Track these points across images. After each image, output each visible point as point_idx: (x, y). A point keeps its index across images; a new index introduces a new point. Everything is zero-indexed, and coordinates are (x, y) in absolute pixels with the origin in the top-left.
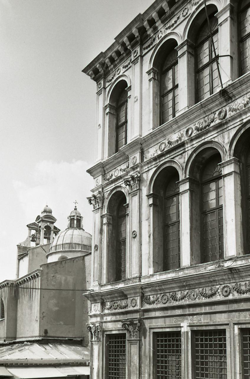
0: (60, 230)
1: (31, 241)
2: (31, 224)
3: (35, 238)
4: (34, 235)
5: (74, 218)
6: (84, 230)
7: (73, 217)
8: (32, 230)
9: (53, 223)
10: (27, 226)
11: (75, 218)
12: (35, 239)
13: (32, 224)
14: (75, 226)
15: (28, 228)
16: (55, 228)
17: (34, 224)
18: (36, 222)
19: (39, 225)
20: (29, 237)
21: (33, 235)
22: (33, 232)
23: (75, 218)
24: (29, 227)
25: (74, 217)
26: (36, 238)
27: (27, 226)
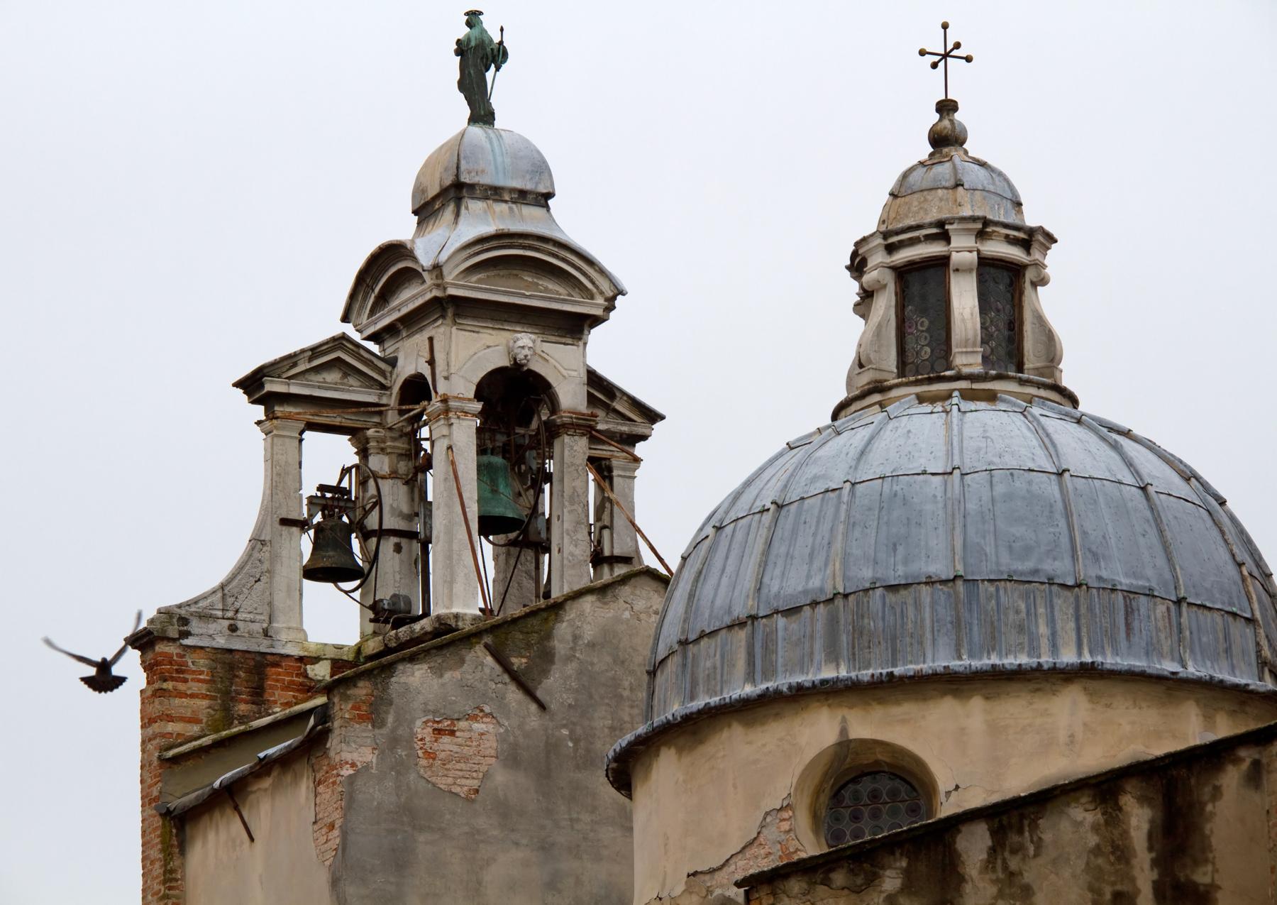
0: (653, 417)
1: (312, 573)
2: (291, 359)
3: (349, 529)
4: (336, 489)
5: (942, 262)
6: (1074, 401)
7: (935, 249)
8: (308, 435)
10: (251, 385)
11: (963, 249)
12: (356, 544)
13: (315, 351)
14: (968, 360)
15: (259, 411)
18: (349, 330)
19: (393, 362)
20: (285, 522)
24: (269, 401)
25: (945, 237)
26: (365, 535)
27: (251, 385)
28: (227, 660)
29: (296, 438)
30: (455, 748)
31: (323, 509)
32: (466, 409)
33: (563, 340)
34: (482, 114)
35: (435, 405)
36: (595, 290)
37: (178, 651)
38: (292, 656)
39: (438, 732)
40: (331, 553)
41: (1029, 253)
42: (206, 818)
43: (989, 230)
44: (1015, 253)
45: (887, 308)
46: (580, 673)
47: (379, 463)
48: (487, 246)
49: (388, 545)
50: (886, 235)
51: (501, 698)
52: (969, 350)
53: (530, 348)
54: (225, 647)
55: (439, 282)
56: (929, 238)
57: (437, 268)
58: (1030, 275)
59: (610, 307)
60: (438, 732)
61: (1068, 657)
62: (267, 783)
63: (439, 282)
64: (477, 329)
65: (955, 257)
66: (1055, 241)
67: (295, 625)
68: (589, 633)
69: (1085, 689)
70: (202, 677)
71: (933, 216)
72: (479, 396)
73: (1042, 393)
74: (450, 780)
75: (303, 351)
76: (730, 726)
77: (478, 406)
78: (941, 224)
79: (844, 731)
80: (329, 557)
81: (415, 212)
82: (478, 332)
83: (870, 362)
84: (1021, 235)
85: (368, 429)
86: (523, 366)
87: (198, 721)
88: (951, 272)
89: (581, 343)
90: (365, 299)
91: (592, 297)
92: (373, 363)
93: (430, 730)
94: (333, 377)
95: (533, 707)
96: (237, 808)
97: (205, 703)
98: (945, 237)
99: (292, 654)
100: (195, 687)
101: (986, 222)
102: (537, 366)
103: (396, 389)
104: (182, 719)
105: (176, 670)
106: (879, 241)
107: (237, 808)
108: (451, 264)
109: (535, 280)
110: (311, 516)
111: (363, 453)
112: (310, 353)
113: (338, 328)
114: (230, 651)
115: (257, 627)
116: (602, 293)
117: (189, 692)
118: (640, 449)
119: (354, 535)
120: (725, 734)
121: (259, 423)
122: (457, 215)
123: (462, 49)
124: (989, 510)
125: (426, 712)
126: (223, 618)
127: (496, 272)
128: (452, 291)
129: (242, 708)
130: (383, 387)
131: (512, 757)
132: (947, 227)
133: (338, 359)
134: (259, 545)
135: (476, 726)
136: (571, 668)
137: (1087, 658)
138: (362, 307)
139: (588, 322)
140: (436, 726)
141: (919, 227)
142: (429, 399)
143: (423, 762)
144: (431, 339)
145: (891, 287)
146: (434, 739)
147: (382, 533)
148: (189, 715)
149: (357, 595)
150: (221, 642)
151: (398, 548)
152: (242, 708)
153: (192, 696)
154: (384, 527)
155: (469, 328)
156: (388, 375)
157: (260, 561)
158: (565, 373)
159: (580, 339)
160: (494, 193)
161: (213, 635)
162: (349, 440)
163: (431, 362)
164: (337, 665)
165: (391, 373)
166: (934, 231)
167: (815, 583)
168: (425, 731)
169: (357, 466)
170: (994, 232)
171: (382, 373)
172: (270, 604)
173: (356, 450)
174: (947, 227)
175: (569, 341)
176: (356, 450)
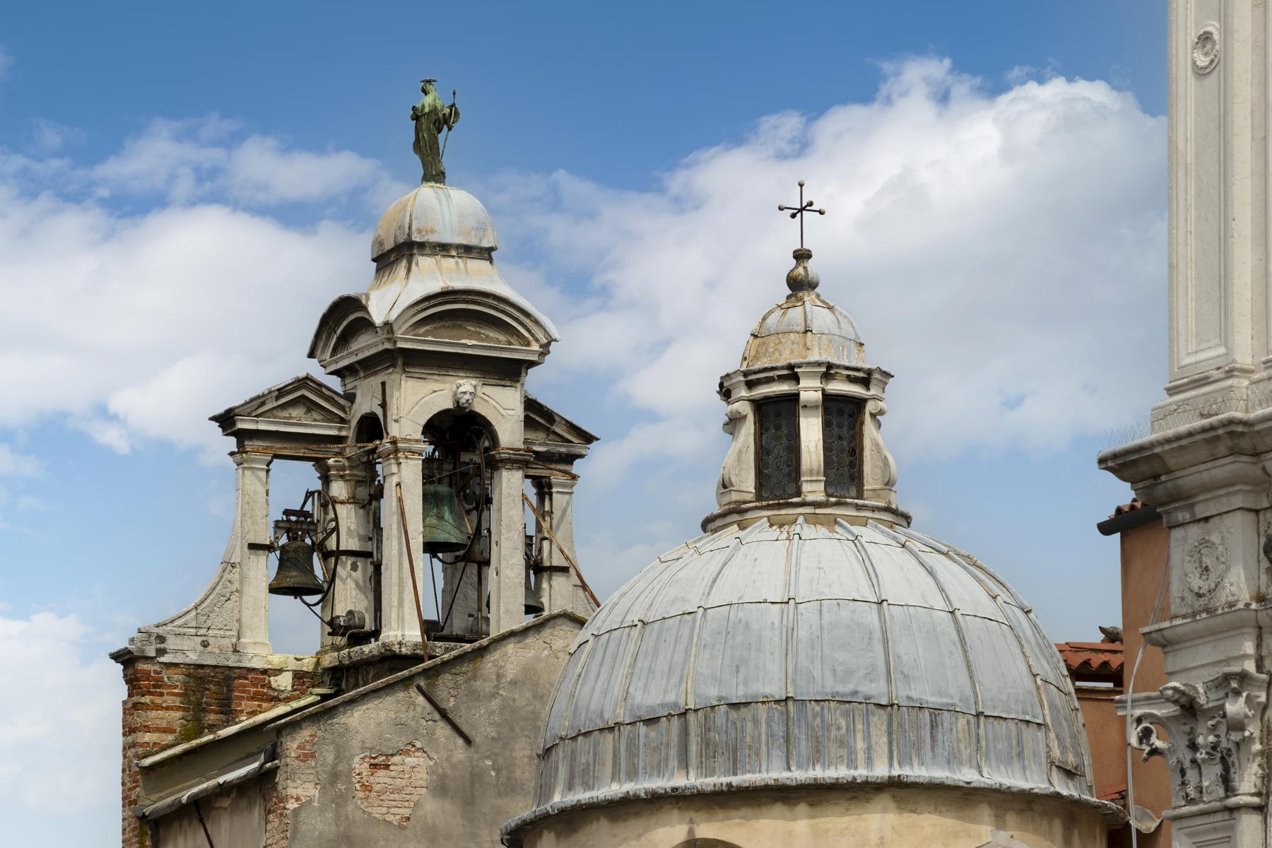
0: (588, 438)
2: (260, 400)
4: (301, 513)
5: (795, 397)
10: (226, 420)
11: (810, 390)
13: (281, 392)
15: (232, 443)
16: (536, 414)
19: (351, 397)
20: (253, 547)
23: (810, 390)
24: (242, 436)
25: (795, 378)
26: (326, 555)
27: (226, 420)
29: (263, 469)
30: (389, 781)
31: (288, 531)
32: (413, 449)
33: (503, 383)
35: (385, 445)
36: (531, 338)
37: (157, 668)
38: (258, 669)
39: (374, 766)
40: (294, 574)
41: (868, 389)
42: (176, 824)
43: (832, 372)
44: (856, 390)
46: (503, 708)
47: (339, 489)
48: (433, 302)
50: (745, 374)
51: (431, 733)
52: (814, 478)
53: (471, 393)
54: (198, 663)
55: (390, 336)
56: (782, 378)
57: (388, 326)
58: (870, 407)
59: (545, 350)
60: (374, 766)
61: (881, 771)
63: (390, 336)
64: (424, 376)
65: (804, 396)
67: (260, 640)
68: (511, 672)
69: (894, 797)
70: (176, 691)
73: (877, 515)
74: (384, 810)
75: (270, 392)
76: (598, 819)
79: (691, 831)
80: (292, 577)
81: (374, 260)
82: (425, 379)
83: (732, 485)
84: (861, 375)
85: (329, 459)
86: (465, 408)
87: (172, 731)
88: (800, 408)
89: (518, 385)
90: (328, 339)
91: (528, 344)
92: (334, 399)
93: (367, 765)
94: (297, 412)
95: (460, 741)
96: (202, 821)
97: (179, 714)
98: (795, 378)
99: (258, 667)
100: (170, 700)
101: (830, 366)
102: (479, 408)
103: (354, 423)
104: (158, 730)
105: (154, 685)
107: (202, 821)
108: (401, 321)
109: (478, 329)
111: (326, 479)
112: (277, 393)
113: (302, 365)
114: (202, 666)
115: (227, 643)
116: (537, 340)
117: (164, 705)
118: (577, 467)
119: (315, 554)
120: (595, 826)
121: (232, 454)
122: (409, 270)
124: (818, 637)
125: (363, 749)
126: (196, 635)
127: (443, 323)
128: (400, 345)
129: (212, 717)
130: (343, 421)
131: (440, 788)
132: (796, 370)
133: (303, 396)
134: (230, 568)
135: (408, 760)
136: (495, 704)
137: (896, 772)
138: (326, 345)
139: (526, 365)
140: (372, 761)
141: (773, 369)
142: (381, 438)
143: (361, 794)
144: (383, 384)
145: (751, 418)
146: (370, 773)
147: (338, 553)
148: (164, 725)
149: (318, 609)
150: (193, 658)
152: (212, 717)
153: (167, 708)
154: (341, 549)
155: (417, 375)
156: (347, 410)
157: (230, 581)
158: (503, 412)
159: (518, 381)
160: (443, 249)
161: (186, 651)
162: (313, 465)
164: (299, 676)
165: (350, 408)
166: (785, 372)
167: (671, 698)
168: (362, 766)
169: (319, 493)
170: (836, 373)
172: (239, 621)
173: (319, 475)
174: (796, 370)
175: (508, 383)
176: (319, 475)
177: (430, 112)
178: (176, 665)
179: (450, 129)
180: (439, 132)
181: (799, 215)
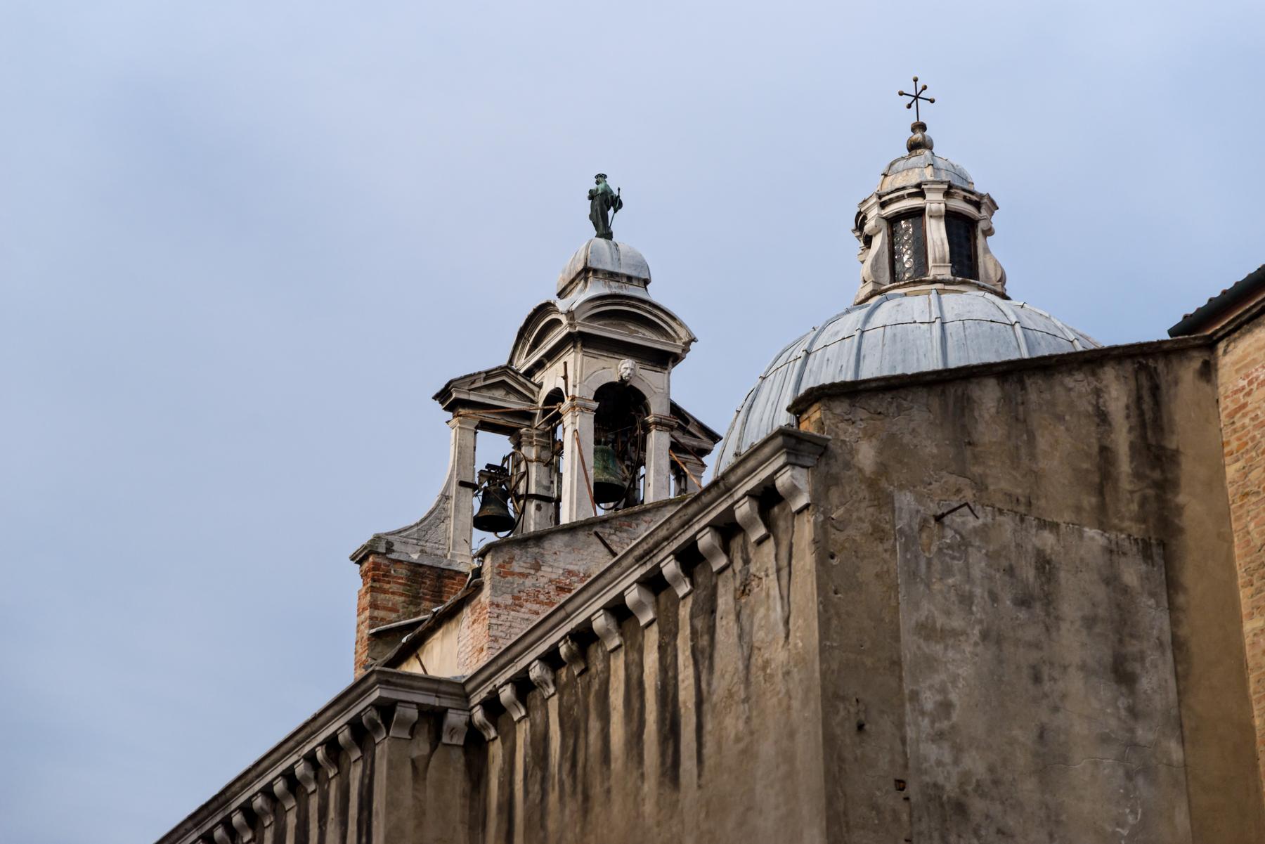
0: (715, 438)
2: (471, 378)
3: (506, 495)
8: (481, 433)
9: (664, 360)
10: (442, 396)
12: (510, 505)
13: (488, 374)
14: (939, 269)
17: (500, 378)
20: (463, 484)
21: (495, 473)
22: (493, 448)
23: (934, 202)
26: (518, 498)
27: (442, 396)
28: (416, 571)
29: (473, 430)
32: (587, 406)
33: (655, 369)
34: (605, 232)
36: (676, 337)
38: (463, 573)
40: (493, 507)
43: (952, 191)
44: (969, 209)
45: (882, 244)
47: (531, 452)
48: (604, 302)
49: (532, 507)
52: (938, 264)
53: (632, 369)
54: (417, 562)
55: (572, 322)
56: (911, 195)
59: (686, 349)
62: (439, 634)
63: (572, 322)
64: (596, 356)
66: (998, 208)
67: (466, 554)
70: (400, 581)
71: (915, 181)
72: (596, 399)
77: (596, 405)
78: (919, 186)
80: (491, 509)
82: (597, 358)
84: (974, 198)
85: (521, 429)
86: (627, 382)
89: (666, 372)
90: (523, 348)
91: (675, 341)
92: (526, 384)
93: (554, 587)
94: (499, 393)
96: (418, 657)
97: (402, 599)
98: (921, 194)
99: (464, 571)
101: (950, 186)
104: (385, 608)
105: (383, 575)
106: (874, 200)
109: (636, 329)
110: (481, 483)
111: (518, 446)
112: (485, 375)
114: (421, 565)
116: (681, 339)
117: (391, 590)
119: (509, 500)
122: (586, 287)
123: (592, 196)
126: (417, 545)
127: (611, 321)
130: (532, 401)
132: (923, 187)
133: (503, 382)
134: (444, 499)
139: (671, 359)
140: (558, 585)
141: (904, 188)
142: (563, 401)
144: (565, 363)
145: (885, 231)
146: (556, 593)
147: (528, 497)
148: (390, 605)
150: (415, 557)
151: (538, 508)
153: (393, 593)
154: (529, 493)
155: (591, 355)
156: (536, 394)
157: (444, 509)
158: (656, 390)
159: (666, 369)
162: (509, 439)
163: (565, 378)
165: (538, 392)
166: (915, 190)
168: (550, 587)
169: (513, 454)
170: (956, 193)
171: (532, 392)
173: (513, 446)
174: (923, 187)
175: (659, 370)
176: (513, 446)
177: (602, 194)
178: (401, 562)
179: (616, 211)
180: (609, 209)
181: (914, 105)
